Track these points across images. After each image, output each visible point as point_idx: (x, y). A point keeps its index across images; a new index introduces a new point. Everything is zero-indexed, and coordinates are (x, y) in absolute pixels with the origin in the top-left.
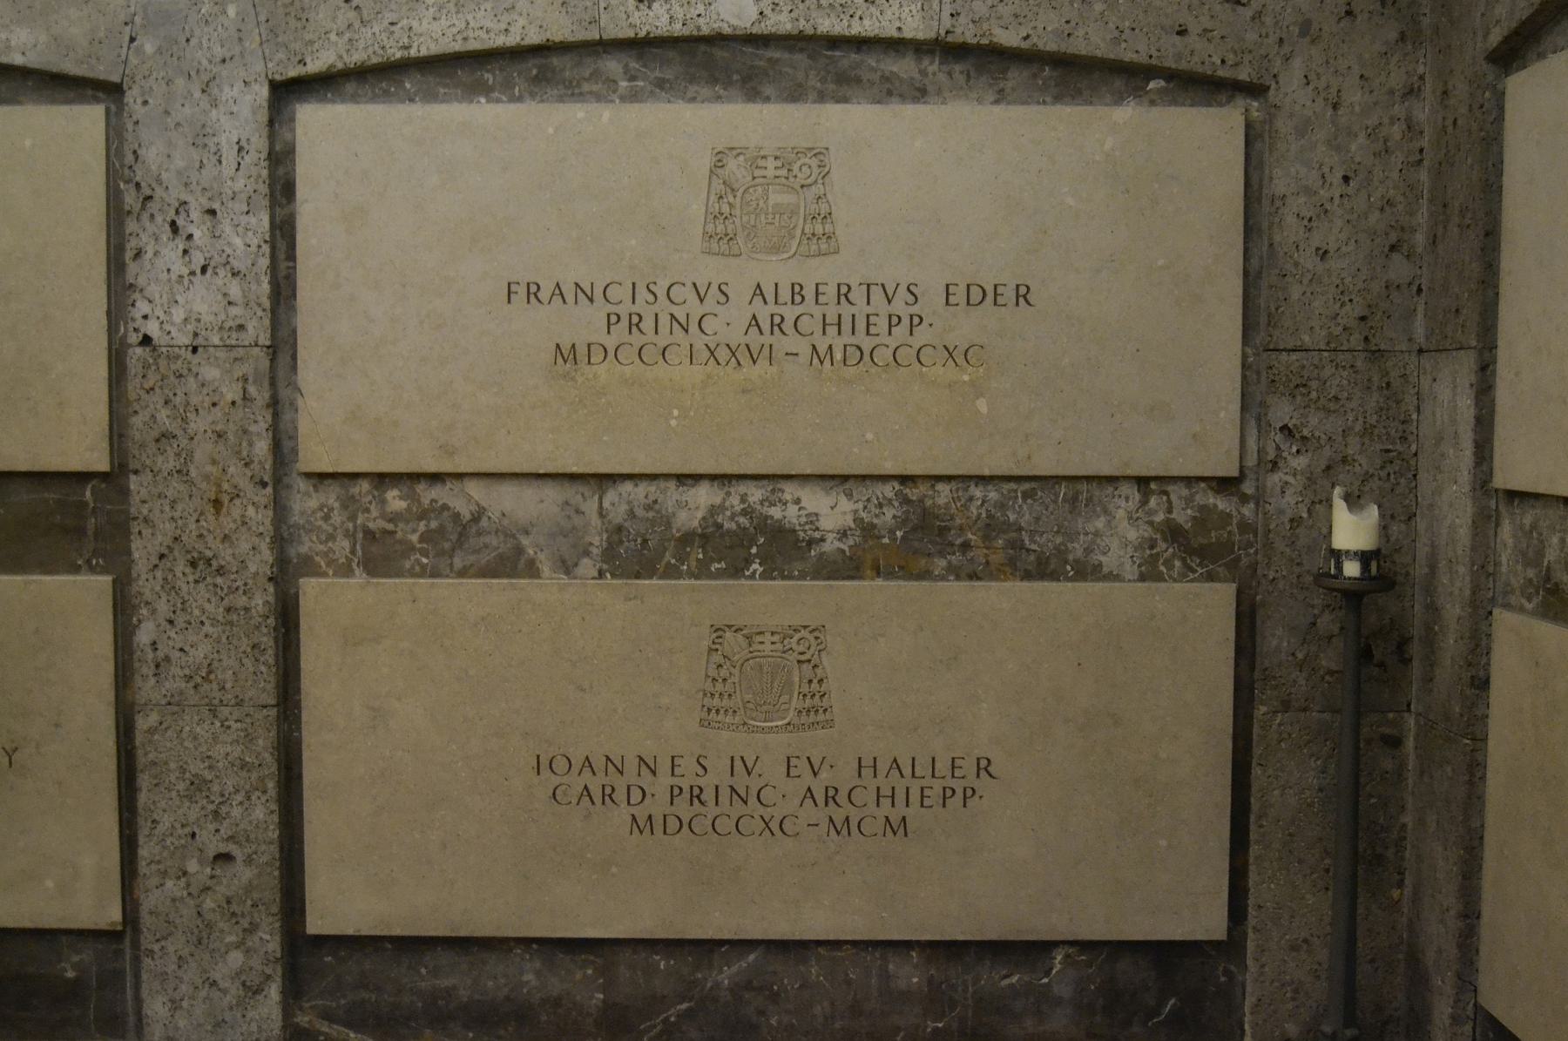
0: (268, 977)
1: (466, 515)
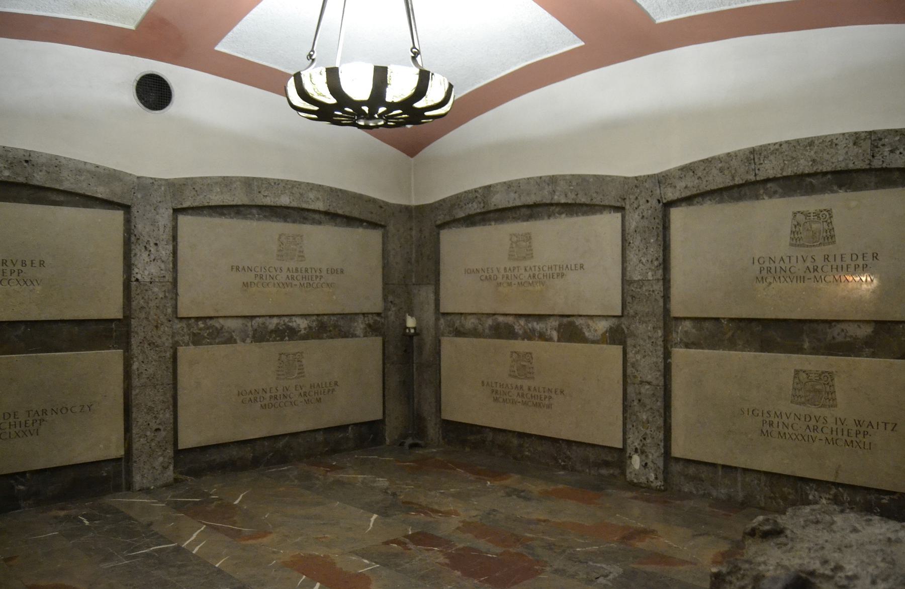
0: (170, 463)
1: (219, 328)
